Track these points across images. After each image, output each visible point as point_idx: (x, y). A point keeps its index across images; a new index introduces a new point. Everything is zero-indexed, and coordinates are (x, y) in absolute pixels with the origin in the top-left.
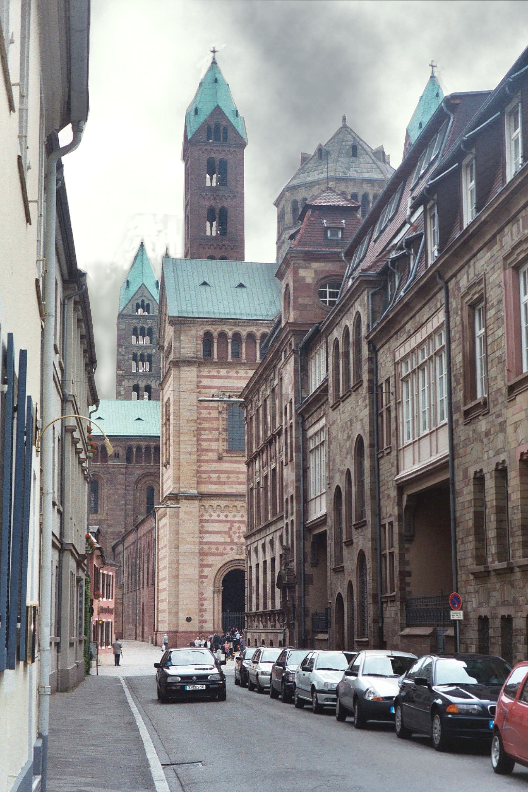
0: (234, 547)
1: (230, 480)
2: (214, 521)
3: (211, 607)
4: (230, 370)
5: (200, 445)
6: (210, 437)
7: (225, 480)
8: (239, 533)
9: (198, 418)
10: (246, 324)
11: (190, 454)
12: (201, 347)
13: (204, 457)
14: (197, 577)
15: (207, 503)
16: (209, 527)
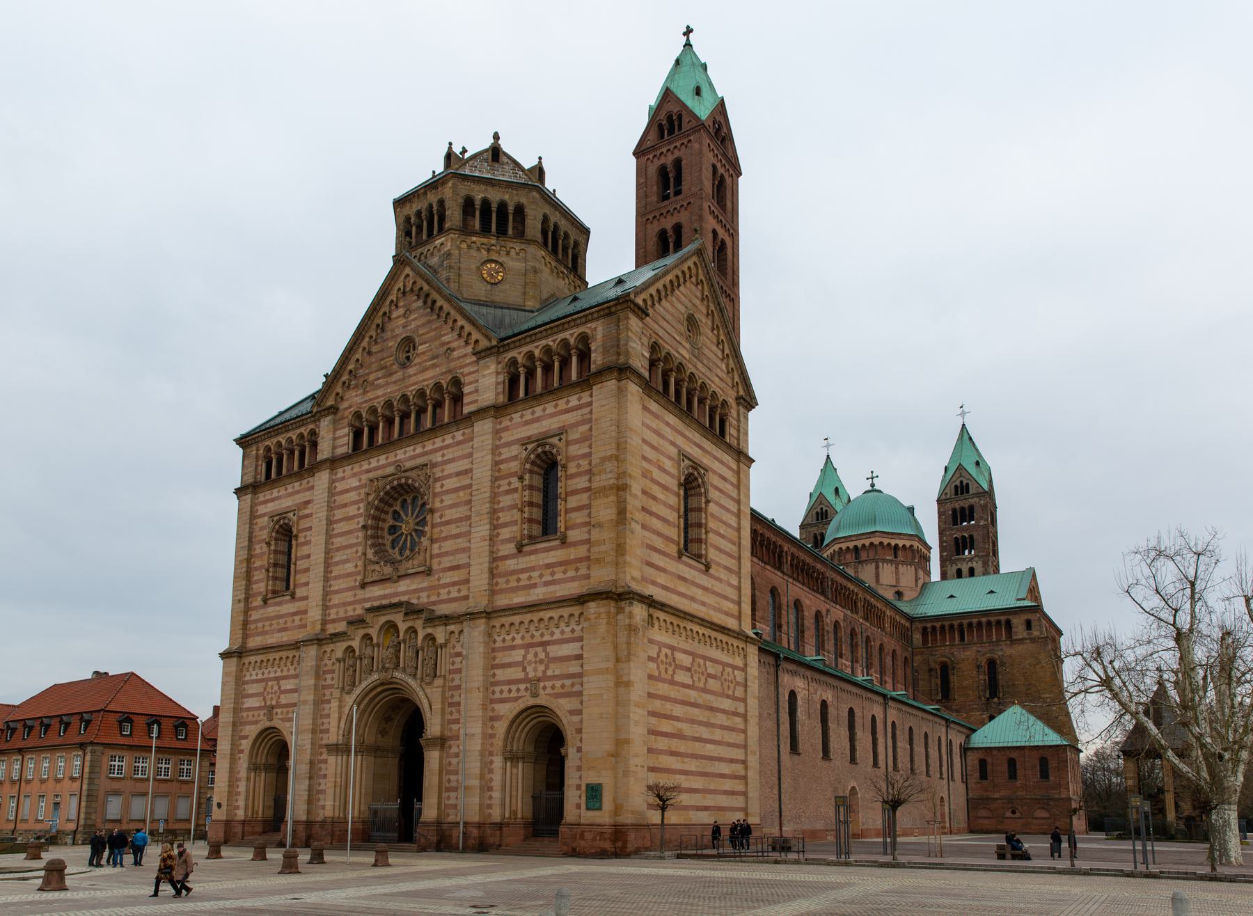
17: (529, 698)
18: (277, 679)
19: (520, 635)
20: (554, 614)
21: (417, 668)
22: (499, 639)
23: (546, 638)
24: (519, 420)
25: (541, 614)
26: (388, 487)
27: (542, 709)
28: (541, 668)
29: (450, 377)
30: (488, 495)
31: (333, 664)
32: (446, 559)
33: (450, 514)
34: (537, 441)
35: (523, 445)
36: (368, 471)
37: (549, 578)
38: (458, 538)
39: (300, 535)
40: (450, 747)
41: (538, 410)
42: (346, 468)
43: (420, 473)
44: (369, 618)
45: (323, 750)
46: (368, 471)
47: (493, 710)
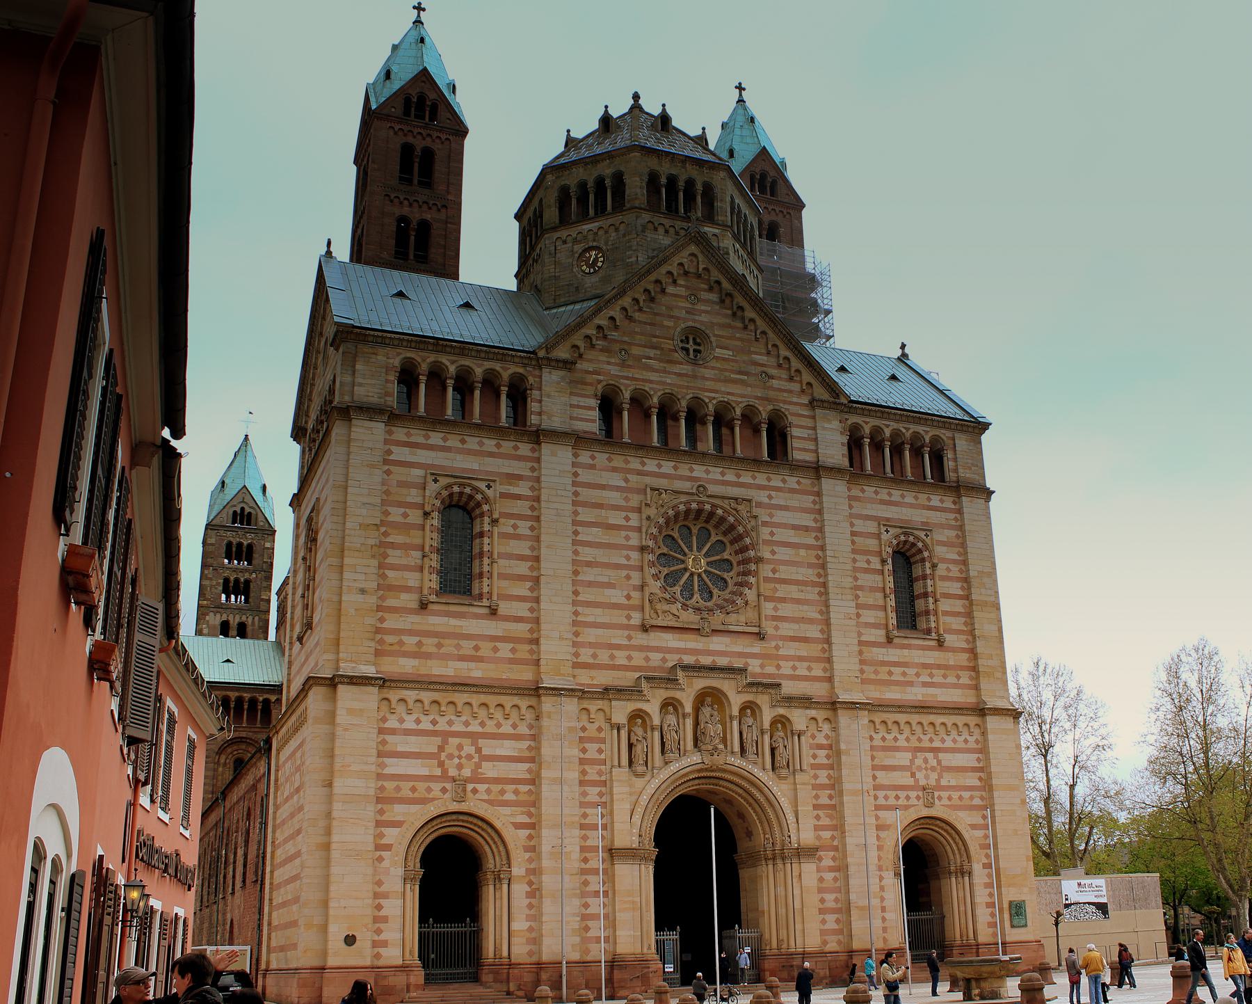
0: (448, 786)
1: (443, 650)
2: (408, 732)
3: (399, 912)
4: (449, 436)
5: (384, 576)
6: (404, 561)
7: (433, 650)
8: (460, 757)
9: (383, 523)
10: (483, 355)
11: (363, 591)
12: (394, 388)
13: (391, 602)
14: (371, 847)
15: (394, 695)
16: (399, 743)
17: (923, 808)
18: (474, 737)
19: (904, 736)
20: (949, 720)
21: (757, 754)
22: (877, 737)
23: (937, 744)
24: (874, 496)
25: (932, 718)
26: (682, 507)
27: (933, 821)
28: (934, 776)
29: (771, 407)
30: (849, 567)
31: (600, 729)
32: (786, 625)
33: (785, 572)
34: (901, 527)
35: (884, 525)
36: (640, 473)
37: (928, 679)
38: (803, 604)
39: (502, 520)
40: (820, 859)
41: (896, 495)
42: (596, 454)
43: (739, 507)
44: (680, 674)
45: (587, 855)
46: (640, 473)
47: (877, 818)
